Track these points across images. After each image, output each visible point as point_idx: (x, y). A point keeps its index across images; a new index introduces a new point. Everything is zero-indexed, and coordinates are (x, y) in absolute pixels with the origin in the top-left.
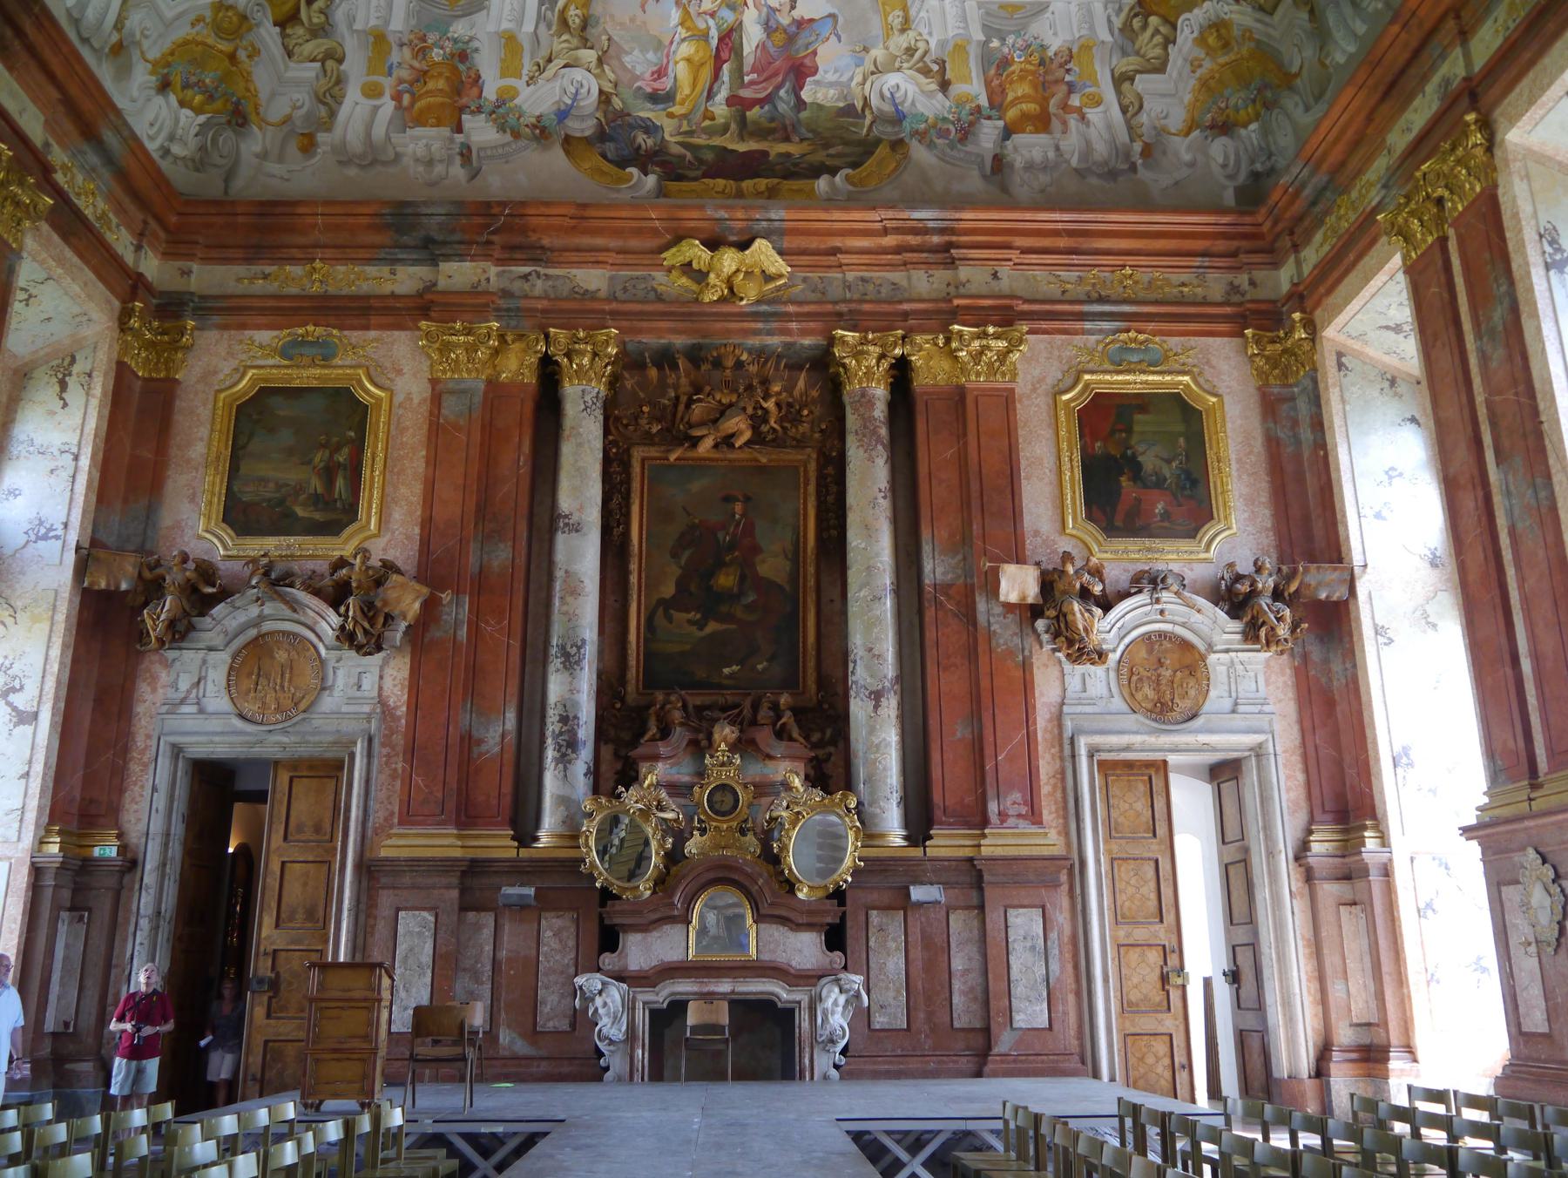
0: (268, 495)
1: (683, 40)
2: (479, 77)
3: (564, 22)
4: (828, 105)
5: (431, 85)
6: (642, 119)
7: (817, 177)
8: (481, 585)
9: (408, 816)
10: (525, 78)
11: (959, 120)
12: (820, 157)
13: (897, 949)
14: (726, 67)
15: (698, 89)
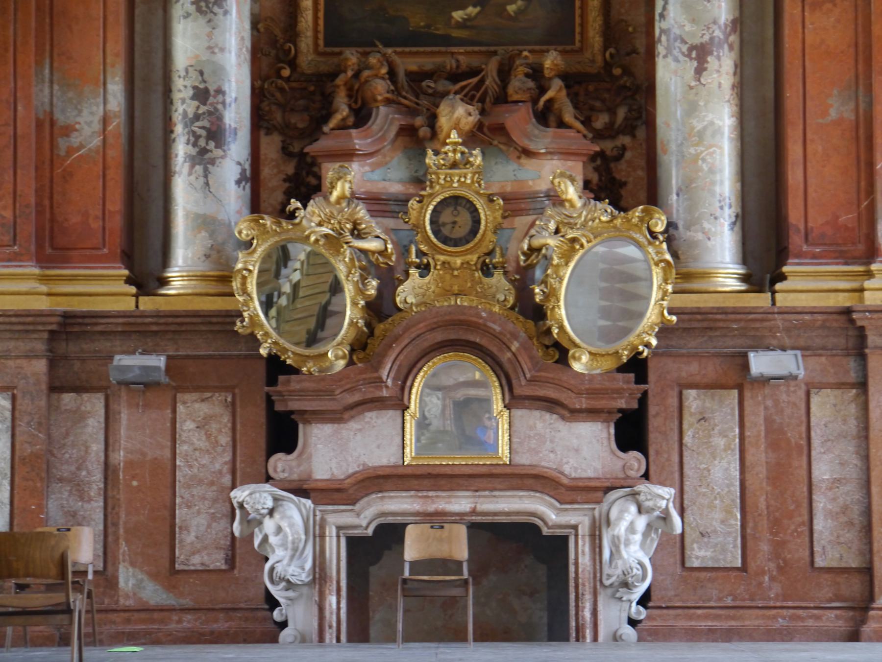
13: (727, 448)
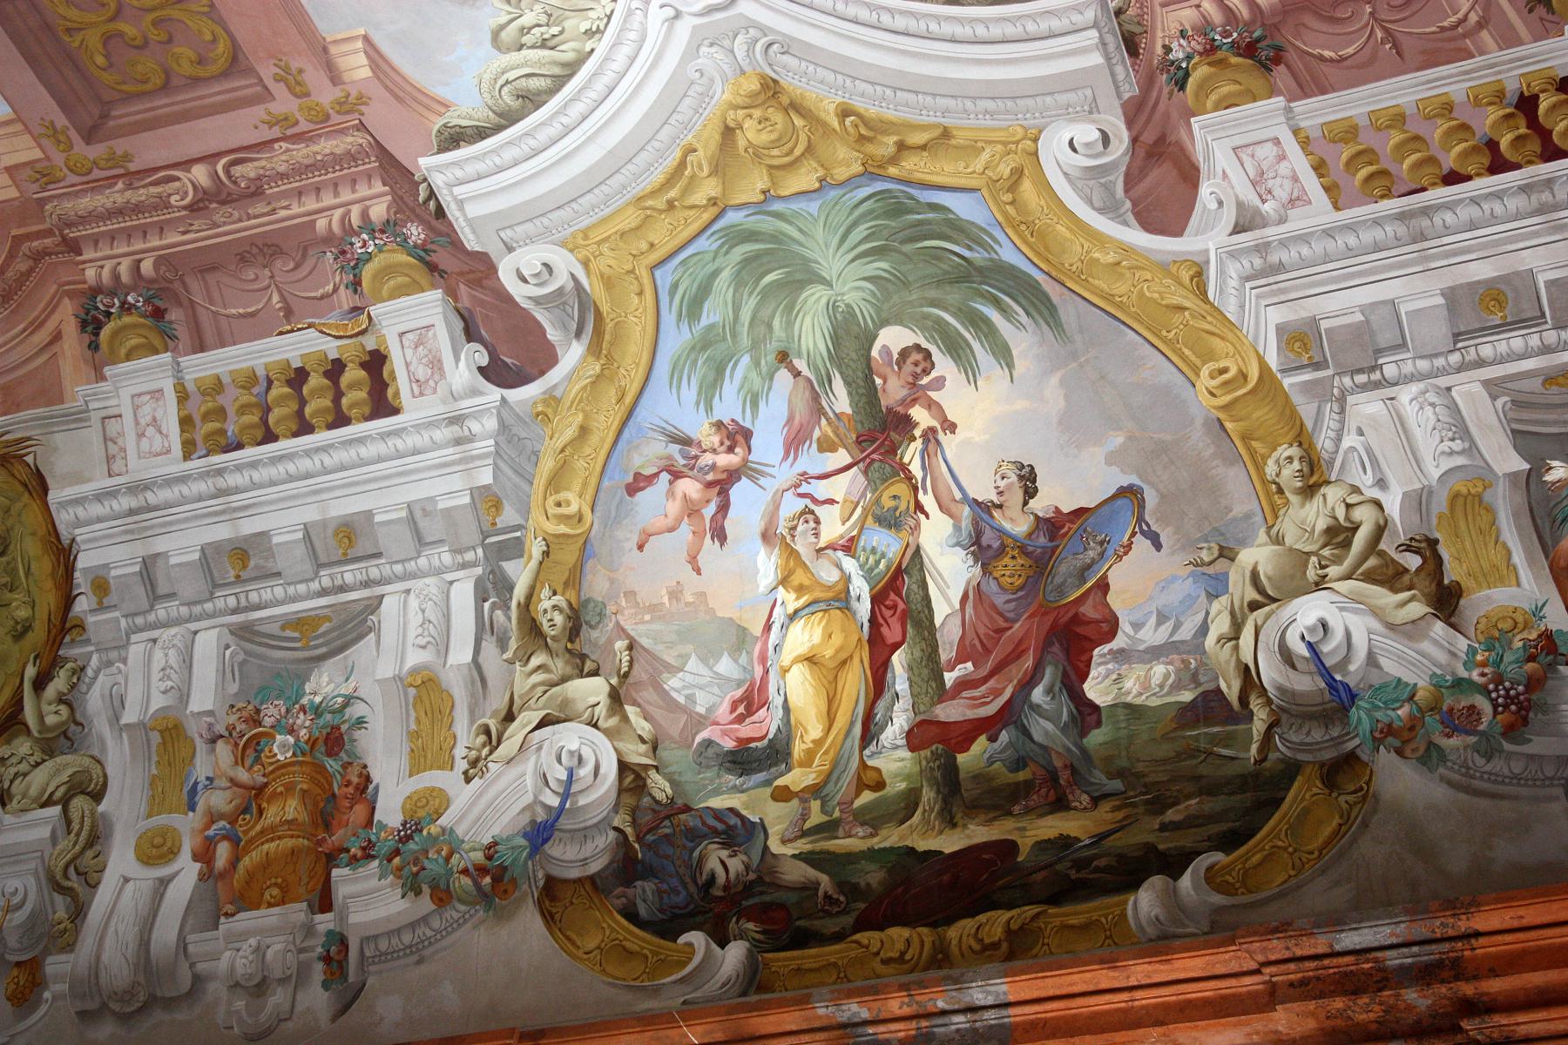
1: (793, 617)
2: (368, 779)
3: (532, 629)
4: (1154, 702)
5: (272, 814)
6: (717, 814)
7: (1134, 885)
10: (461, 765)
11: (1498, 679)
12: (1145, 832)
14: (898, 660)
15: (841, 721)
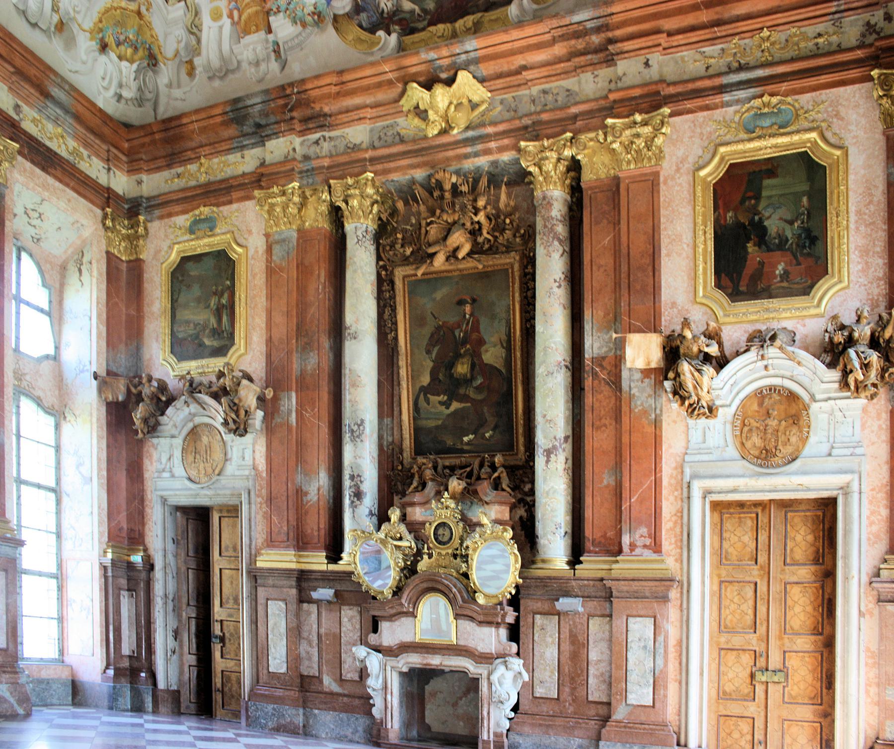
0: (191, 332)
8: (303, 385)
9: (271, 543)
13: (553, 643)
